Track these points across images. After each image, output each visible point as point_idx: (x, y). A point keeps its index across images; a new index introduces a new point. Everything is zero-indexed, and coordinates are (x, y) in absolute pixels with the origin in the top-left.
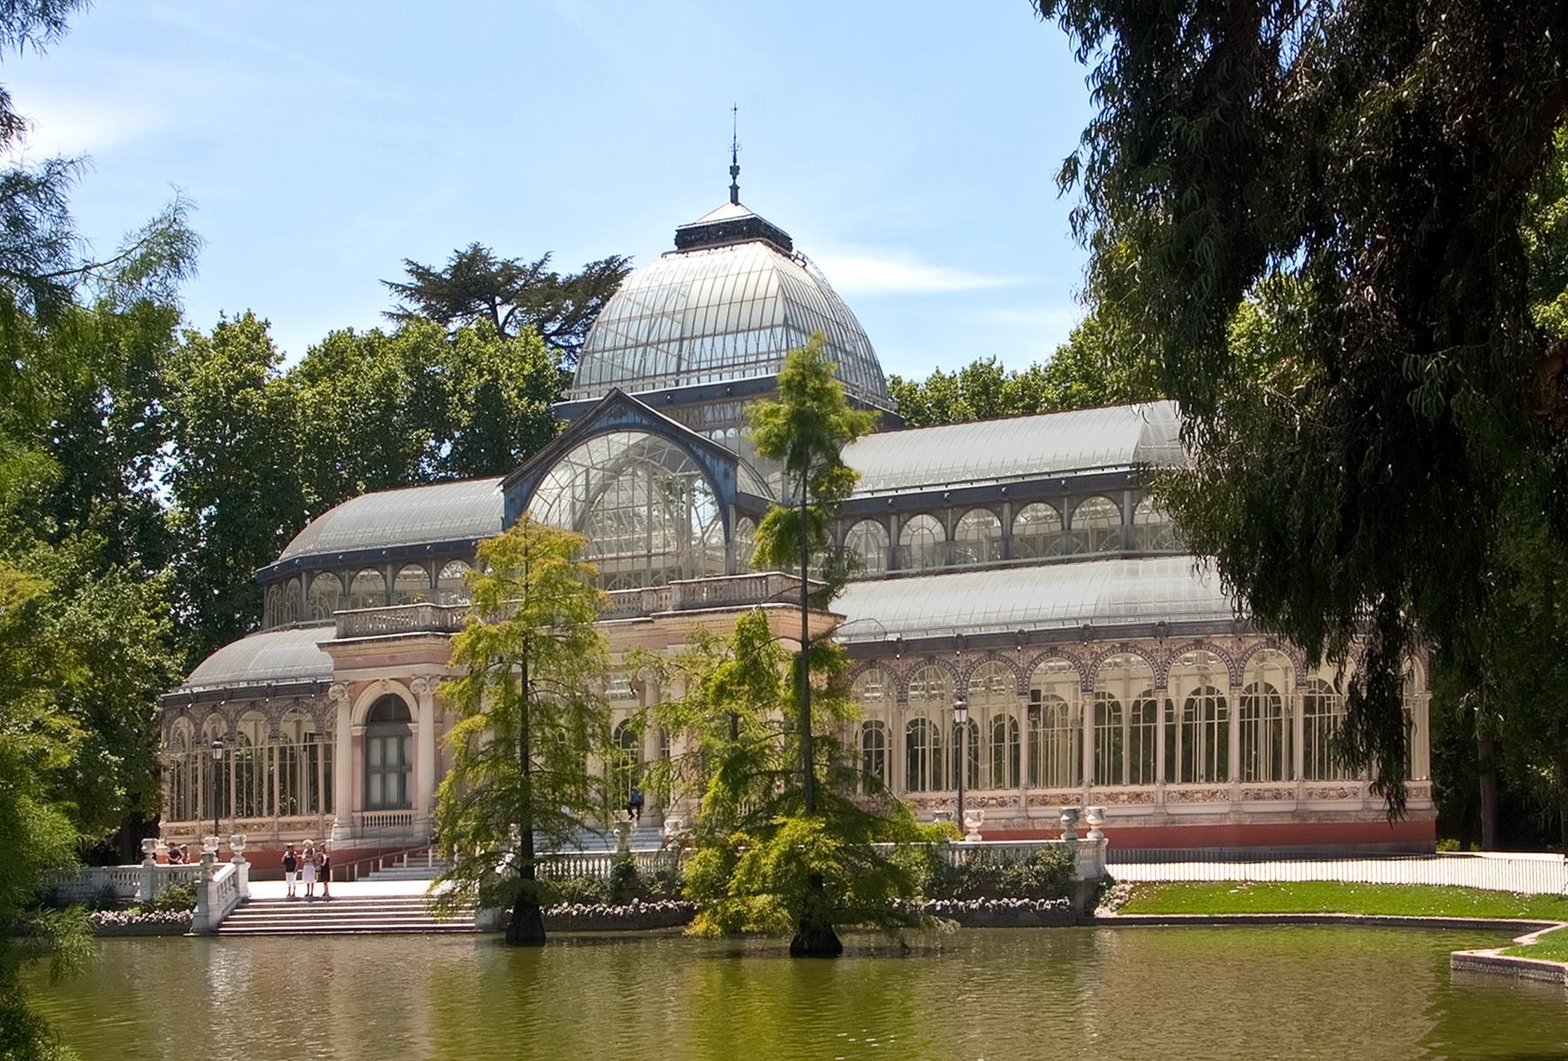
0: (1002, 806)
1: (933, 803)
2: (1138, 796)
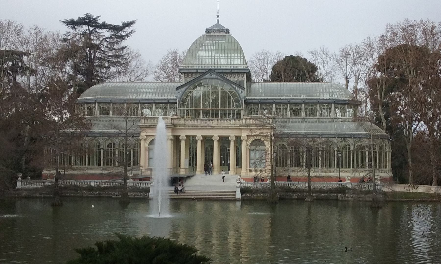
2: (347, 171)
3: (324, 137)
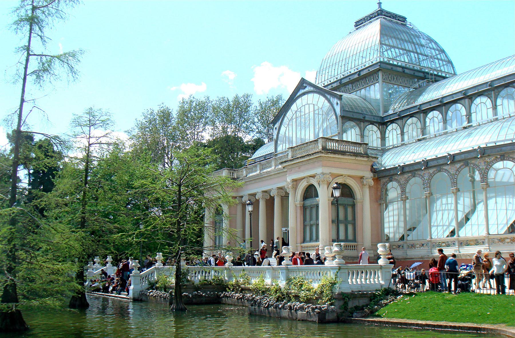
0: (447, 247)
1: (418, 246)
3: (459, 161)
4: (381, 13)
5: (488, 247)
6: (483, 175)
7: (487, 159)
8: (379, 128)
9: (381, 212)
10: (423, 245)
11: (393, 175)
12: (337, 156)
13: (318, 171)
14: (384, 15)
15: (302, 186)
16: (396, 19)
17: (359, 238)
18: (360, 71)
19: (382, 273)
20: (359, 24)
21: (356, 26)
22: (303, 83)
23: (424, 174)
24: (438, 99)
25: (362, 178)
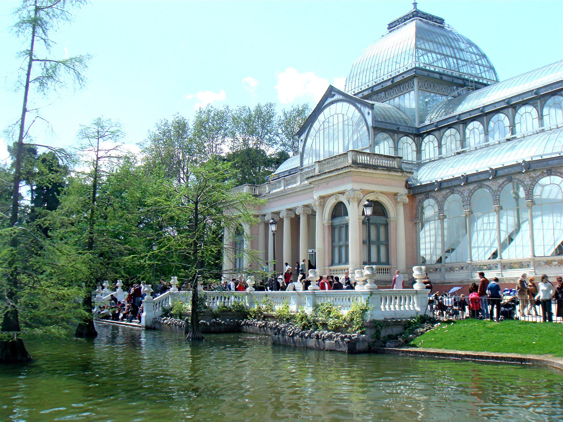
0: (489, 270)
1: (457, 269)
3: (502, 176)
4: (416, 14)
5: (534, 271)
6: (528, 192)
7: (533, 174)
8: (414, 141)
9: (416, 232)
10: (462, 268)
11: (430, 191)
12: (368, 171)
13: (348, 187)
14: (420, 17)
15: (331, 203)
16: (432, 21)
17: (392, 260)
18: (393, 78)
19: (417, 298)
20: (392, 26)
21: (389, 28)
22: (331, 91)
23: (464, 190)
24: (479, 109)
25: (396, 194)
